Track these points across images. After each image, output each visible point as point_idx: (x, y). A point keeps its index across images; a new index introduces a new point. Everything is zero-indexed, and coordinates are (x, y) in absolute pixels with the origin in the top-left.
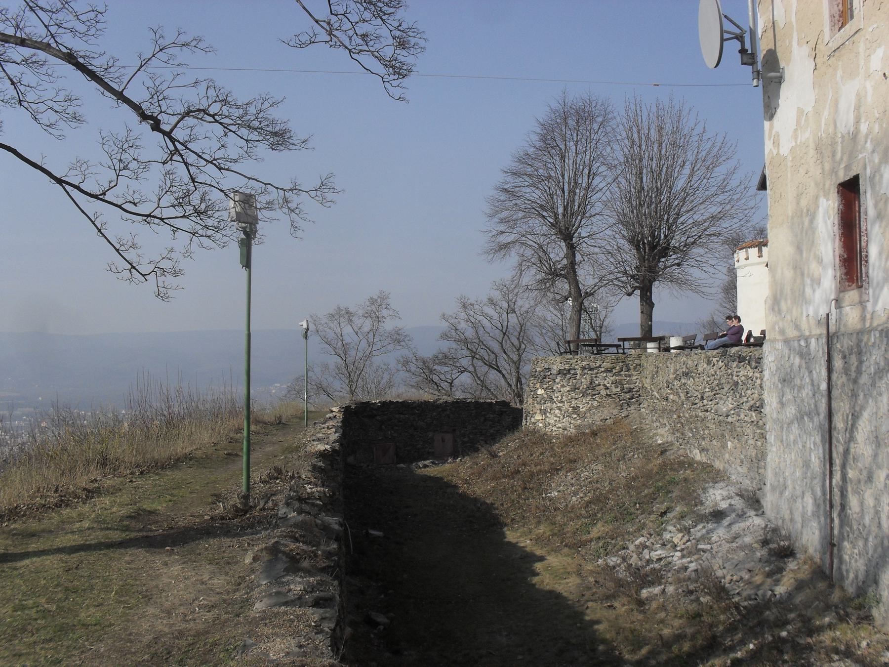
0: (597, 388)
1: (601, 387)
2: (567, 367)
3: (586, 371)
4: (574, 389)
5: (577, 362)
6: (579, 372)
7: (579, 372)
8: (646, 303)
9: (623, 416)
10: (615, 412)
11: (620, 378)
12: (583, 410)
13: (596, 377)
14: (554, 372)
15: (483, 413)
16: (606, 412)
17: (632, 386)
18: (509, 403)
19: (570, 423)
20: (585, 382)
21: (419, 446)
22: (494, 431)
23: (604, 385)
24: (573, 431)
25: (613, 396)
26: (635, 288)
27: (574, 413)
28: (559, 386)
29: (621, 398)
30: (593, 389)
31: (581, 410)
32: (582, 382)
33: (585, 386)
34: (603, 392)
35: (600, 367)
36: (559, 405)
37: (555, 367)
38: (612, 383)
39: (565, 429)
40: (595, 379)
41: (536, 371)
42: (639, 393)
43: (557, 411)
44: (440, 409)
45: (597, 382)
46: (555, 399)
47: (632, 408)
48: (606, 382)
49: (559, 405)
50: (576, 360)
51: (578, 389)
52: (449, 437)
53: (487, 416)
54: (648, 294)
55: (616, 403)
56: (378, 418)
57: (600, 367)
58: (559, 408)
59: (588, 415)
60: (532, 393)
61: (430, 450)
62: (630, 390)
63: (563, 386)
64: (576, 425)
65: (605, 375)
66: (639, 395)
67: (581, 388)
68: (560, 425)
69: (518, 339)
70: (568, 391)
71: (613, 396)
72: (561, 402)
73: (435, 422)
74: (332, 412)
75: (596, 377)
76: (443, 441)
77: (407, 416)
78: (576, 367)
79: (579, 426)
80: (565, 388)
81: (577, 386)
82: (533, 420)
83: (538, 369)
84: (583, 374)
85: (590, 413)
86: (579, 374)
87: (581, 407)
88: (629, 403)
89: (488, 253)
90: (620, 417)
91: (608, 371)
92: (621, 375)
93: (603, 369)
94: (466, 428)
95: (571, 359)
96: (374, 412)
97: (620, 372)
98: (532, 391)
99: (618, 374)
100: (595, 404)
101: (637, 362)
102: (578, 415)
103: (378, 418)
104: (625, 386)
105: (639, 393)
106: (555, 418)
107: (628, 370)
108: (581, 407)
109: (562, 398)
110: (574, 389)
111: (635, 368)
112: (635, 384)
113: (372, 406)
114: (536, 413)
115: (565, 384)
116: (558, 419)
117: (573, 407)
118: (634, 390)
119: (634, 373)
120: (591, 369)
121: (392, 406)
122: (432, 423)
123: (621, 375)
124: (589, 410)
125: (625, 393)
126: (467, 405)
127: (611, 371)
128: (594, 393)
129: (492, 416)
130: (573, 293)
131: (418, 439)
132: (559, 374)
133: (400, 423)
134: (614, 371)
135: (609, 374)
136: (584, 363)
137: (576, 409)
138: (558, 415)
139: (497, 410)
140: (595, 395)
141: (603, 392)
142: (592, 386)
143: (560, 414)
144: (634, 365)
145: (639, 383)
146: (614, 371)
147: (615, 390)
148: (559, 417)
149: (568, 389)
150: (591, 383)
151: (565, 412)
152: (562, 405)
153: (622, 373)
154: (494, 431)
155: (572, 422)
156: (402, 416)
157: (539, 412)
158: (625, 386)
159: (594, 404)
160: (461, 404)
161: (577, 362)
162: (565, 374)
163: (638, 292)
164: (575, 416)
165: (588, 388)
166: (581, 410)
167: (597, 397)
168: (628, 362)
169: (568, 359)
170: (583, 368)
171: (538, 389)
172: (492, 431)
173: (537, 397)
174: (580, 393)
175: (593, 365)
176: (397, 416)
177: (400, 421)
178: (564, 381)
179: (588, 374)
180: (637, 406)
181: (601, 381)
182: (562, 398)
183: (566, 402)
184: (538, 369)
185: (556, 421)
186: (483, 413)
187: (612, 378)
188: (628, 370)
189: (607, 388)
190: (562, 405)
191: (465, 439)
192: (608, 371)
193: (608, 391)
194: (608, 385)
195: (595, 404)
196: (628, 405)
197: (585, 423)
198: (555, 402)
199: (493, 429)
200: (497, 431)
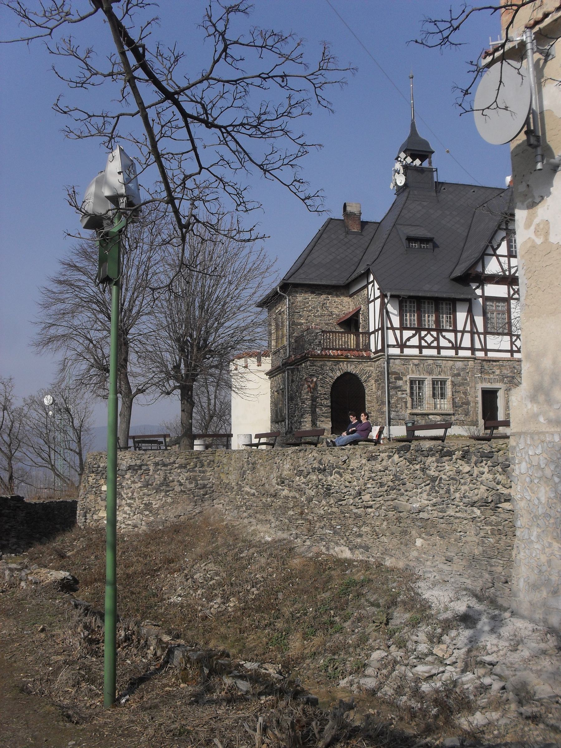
0: (171, 484)
1: (175, 483)
2: (138, 462)
3: (159, 467)
4: (147, 485)
5: (149, 457)
6: (151, 468)
7: (151, 468)
8: (187, 401)
9: (197, 511)
10: (189, 508)
11: (194, 474)
12: (157, 506)
13: (170, 473)
14: (124, 468)
16: (180, 508)
17: (206, 482)
18: (23, 498)
19: (142, 520)
20: (158, 478)
22: (9, 526)
23: (178, 481)
24: (144, 528)
25: (188, 492)
26: (175, 388)
27: (146, 509)
28: (129, 482)
29: (195, 494)
30: (168, 486)
31: (154, 507)
32: (155, 478)
33: (159, 482)
34: (178, 489)
35: (174, 462)
36: (129, 501)
37: (124, 463)
38: (186, 480)
39: (135, 526)
40: (168, 475)
41: (99, 467)
42: (212, 489)
43: (126, 508)
45: (171, 478)
46: (125, 496)
47: (206, 504)
48: (180, 479)
49: (129, 501)
50: (148, 456)
51: (152, 485)
54: (190, 393)
55: (190, 499)
57: (174, 462)
58: (130, 505)
59: (161, 511)
60: (94, 489)
62: (204, 486)
63: (134, 482)
64: (148, 522)
65: (179, 471)
66: (213, 491)
67: (154, 484)
68: (130, 522)
69: (9, 435)
70: (140, 487)
71: (188, 492)
72: (131, 498)
75: (170, 473)
78: (149, 463)
79: (151, 522)
80: (136, 484)
81: (150, 482)
82: (95, 517)
83: (102, 465)
84: (156, 470)
85: (163, 510)
86: (151, 471)
87: (154, 504)
88: (203, 499)
89: (38, 345)
90: (195, 513)
91: (181, 467)
92: (195, 471)
93: (177, 465)
95: (143, 454)
97: (195, 468)
98: (94, 487)
99: (192, 470)
100: (169, 500)
101: (211, 458)
102: (151, 512)
104: (199, 482)
105: (212, 489)
106: (124, 515)
107: (202, 466)
108: (154, 504)
109: (133, 494)
110: (147, 485)
111: (209, 464)
112: (209, 480)
114: (100, 510)
115: (136, 480)
116: (128, 516)
117: (145, 504)
118: (208, 486)
119: (209, 469)
120: (165, 465)
123: (195, 471)
124: (163, 506)
125: (200, 489)
127: (185, 467)
128: (168, 489)
129: (7, 511)
130: (123, 389)
132: (128, 470)
134: (188, 467)
135: (183, 470)
136: (157, 459)
137: (148, 506)
138: (128, 512)
139: (12, 505)
140: (169, 491)
141: (178, 489)
142: (166, 482)
143: (131, 511)
144: (208, 461)
145: (213, 479)
146: (188, 467)
147: (189, 486)
148: (129, 514)
149: (140, 485)
150: (165, 479)
151: (136, 509)
152: (132, 502)
153: (197, 469)
154: (9, 526)
155: (144, 519)
157: (104, 508)
158: (199, 482)
159: (168, 501)
161: (149, 457)
162: (136, 470)
163: (178, 392)
164: (148, 513)
165: (162, 484)
166: (154, 507)
167: (171, 494)
168: (202, 458)
169: (139, 455)
170: (156, 464)
171: (102, 485)
173: (101, 493)
174: (153, 489)
175: (167, 461)
178: (135, 477)
179: (161, 470)
180: (210, 502)
181: (175, 477)
182: (133, 494)
183: (137, 499)
184: (102, 465)
185: (125, 518)
187: (186, 474)
188: (202, 466)
189: (181, 485)
190: (132, 502)
192: (181, 467)
193: (182, 487)
194: (182, 481)
195: (169, 500)
196: (202, 501)
197: (158, 520)
198: (124, 499)
199: (9, 524)
200: (12, 526)
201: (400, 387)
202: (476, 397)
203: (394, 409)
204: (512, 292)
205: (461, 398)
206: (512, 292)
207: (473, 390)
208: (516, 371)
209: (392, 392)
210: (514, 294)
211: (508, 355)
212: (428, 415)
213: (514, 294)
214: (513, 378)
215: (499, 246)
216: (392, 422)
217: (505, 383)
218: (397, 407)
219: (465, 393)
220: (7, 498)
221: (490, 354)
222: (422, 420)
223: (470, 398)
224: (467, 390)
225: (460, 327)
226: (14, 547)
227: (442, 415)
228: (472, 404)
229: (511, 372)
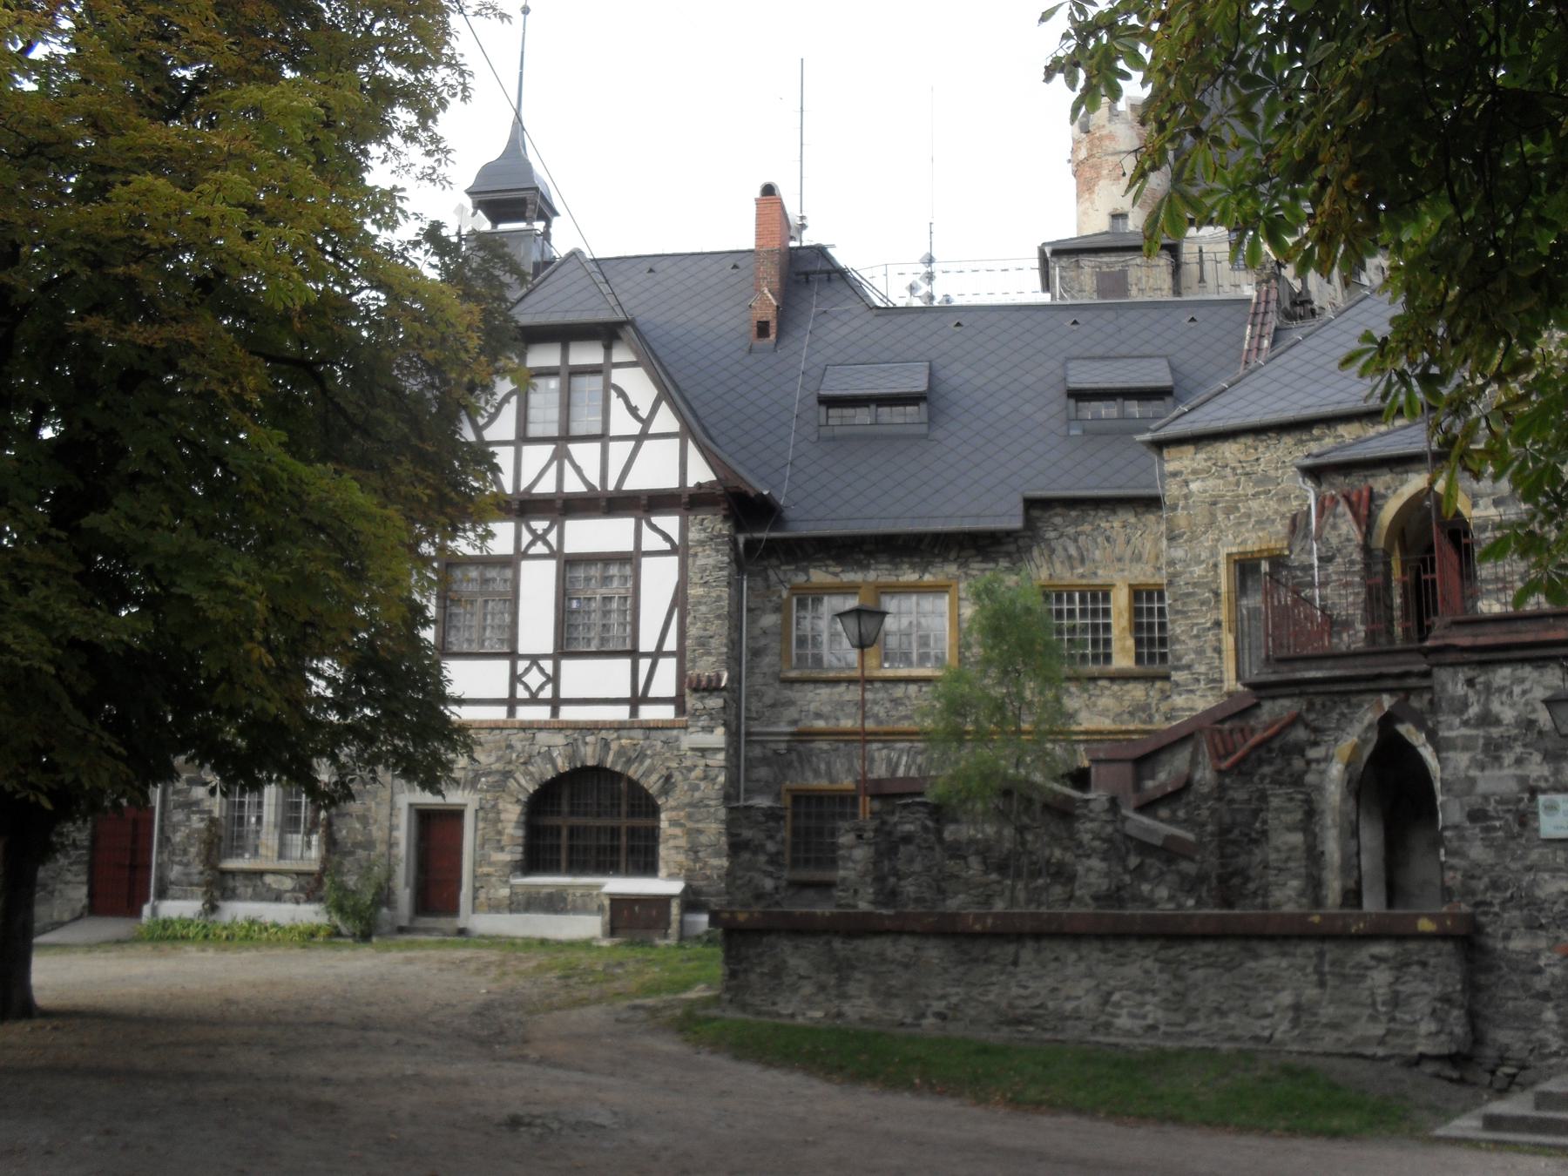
201: (197, 803)
202: (392, 828)
203: (177, 859)
204: (526, 537)
205: (350, 830)
206: (526, 537)
207: (385, 810)
208: (514, 756)
209: (178, 816)
210: (532, 543)
211: (500, 713)
212: (261, 874)
213: (532, 543)
214: (507, 775)
215: (492, 418)
216: (174, 890)
217: (481, 790)
218: (185, 852)
219: (364, 819)
221: (568, 713)
222: (246, 886)
223: (377, 833)
224: (369, 809)
225: (647, 643)
227: (299, 874)
228: (381, 848)
229: (499, 759)
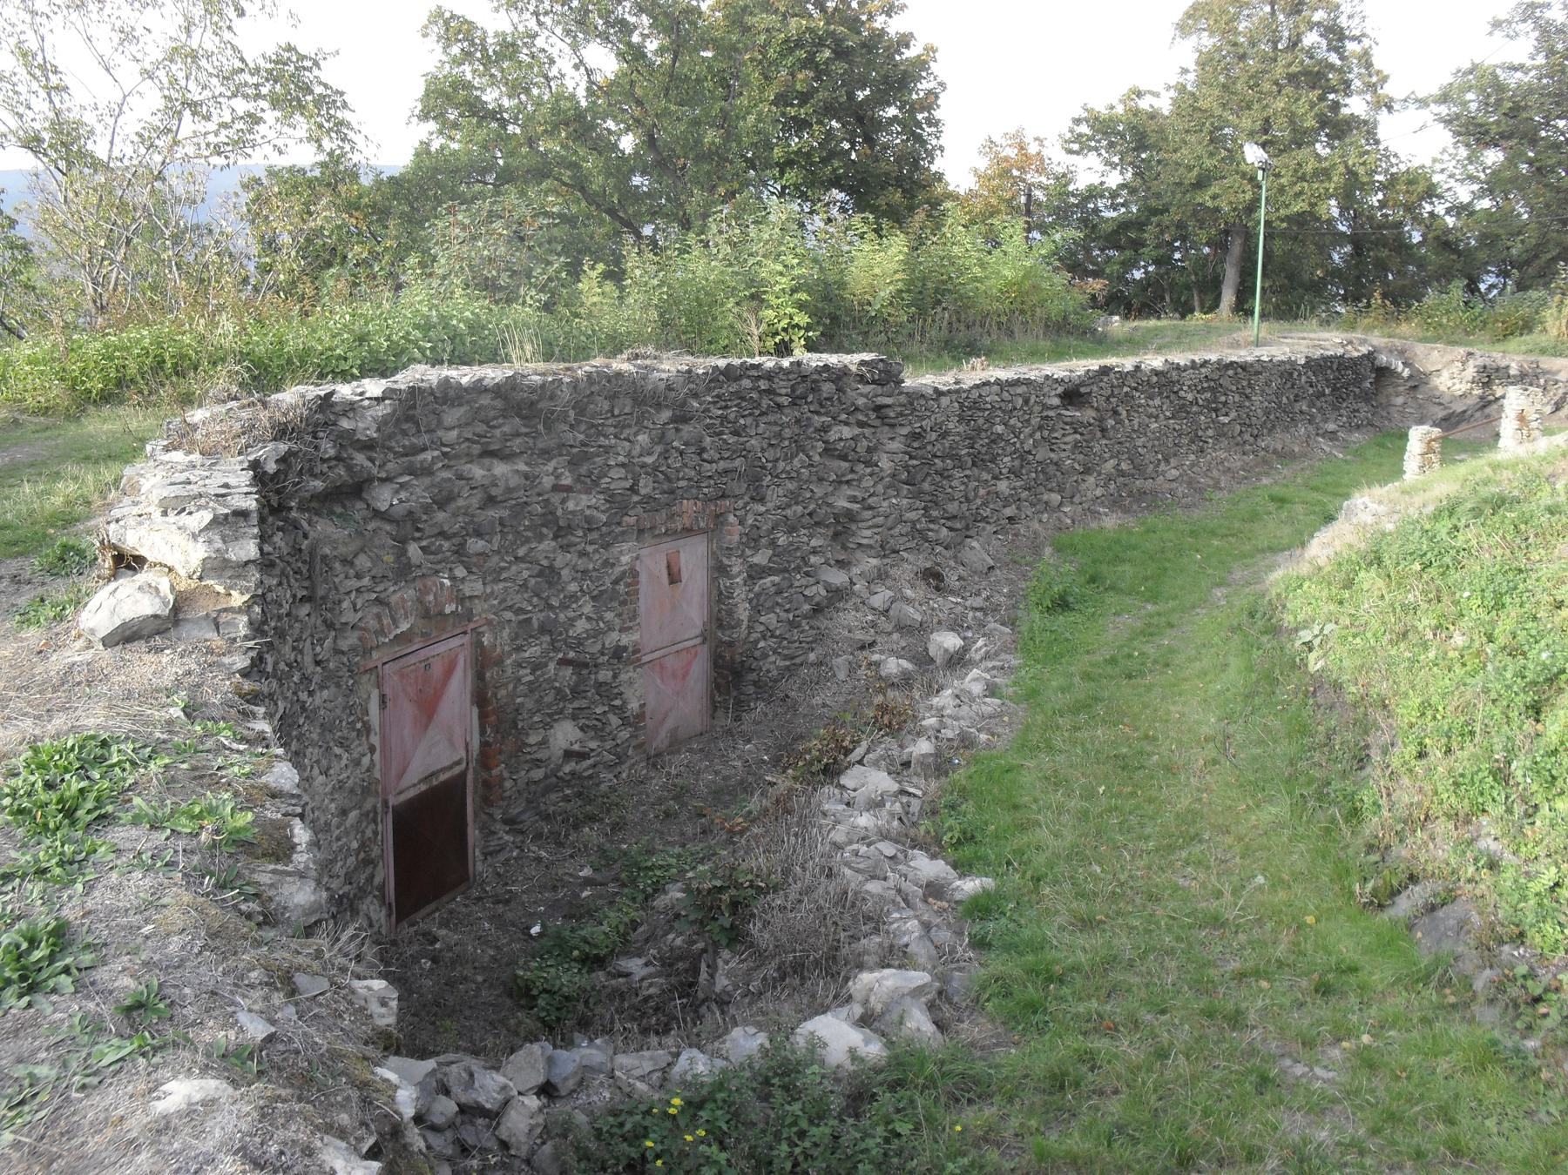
15: (818, 420)
21: (581, 626)
44: (666, 415)
52: (694, 556)
53: (833, 435)
56: (384, 497)
61: (625, 640)
73: (646, 487)
74: (128, 563)
76: (674, 578)
77: (522, 467)
94: (762, 500)
96: (360, 459)
103: (384, 497)
113: (345, 424)
121: (452, 416)
122: (633, 489)
126: (763, 385)
129: (847, 432)
131: (573, 587)
133: (494, 513)
154: (853, 499)
156: (500, 469)
160: (746, 383)
172: (842, 503)
176: (477, 472)
177: (490, 501)
186: (818, 420)
191: (761, 558)
220: (844, 372)
226: (880, 598)
